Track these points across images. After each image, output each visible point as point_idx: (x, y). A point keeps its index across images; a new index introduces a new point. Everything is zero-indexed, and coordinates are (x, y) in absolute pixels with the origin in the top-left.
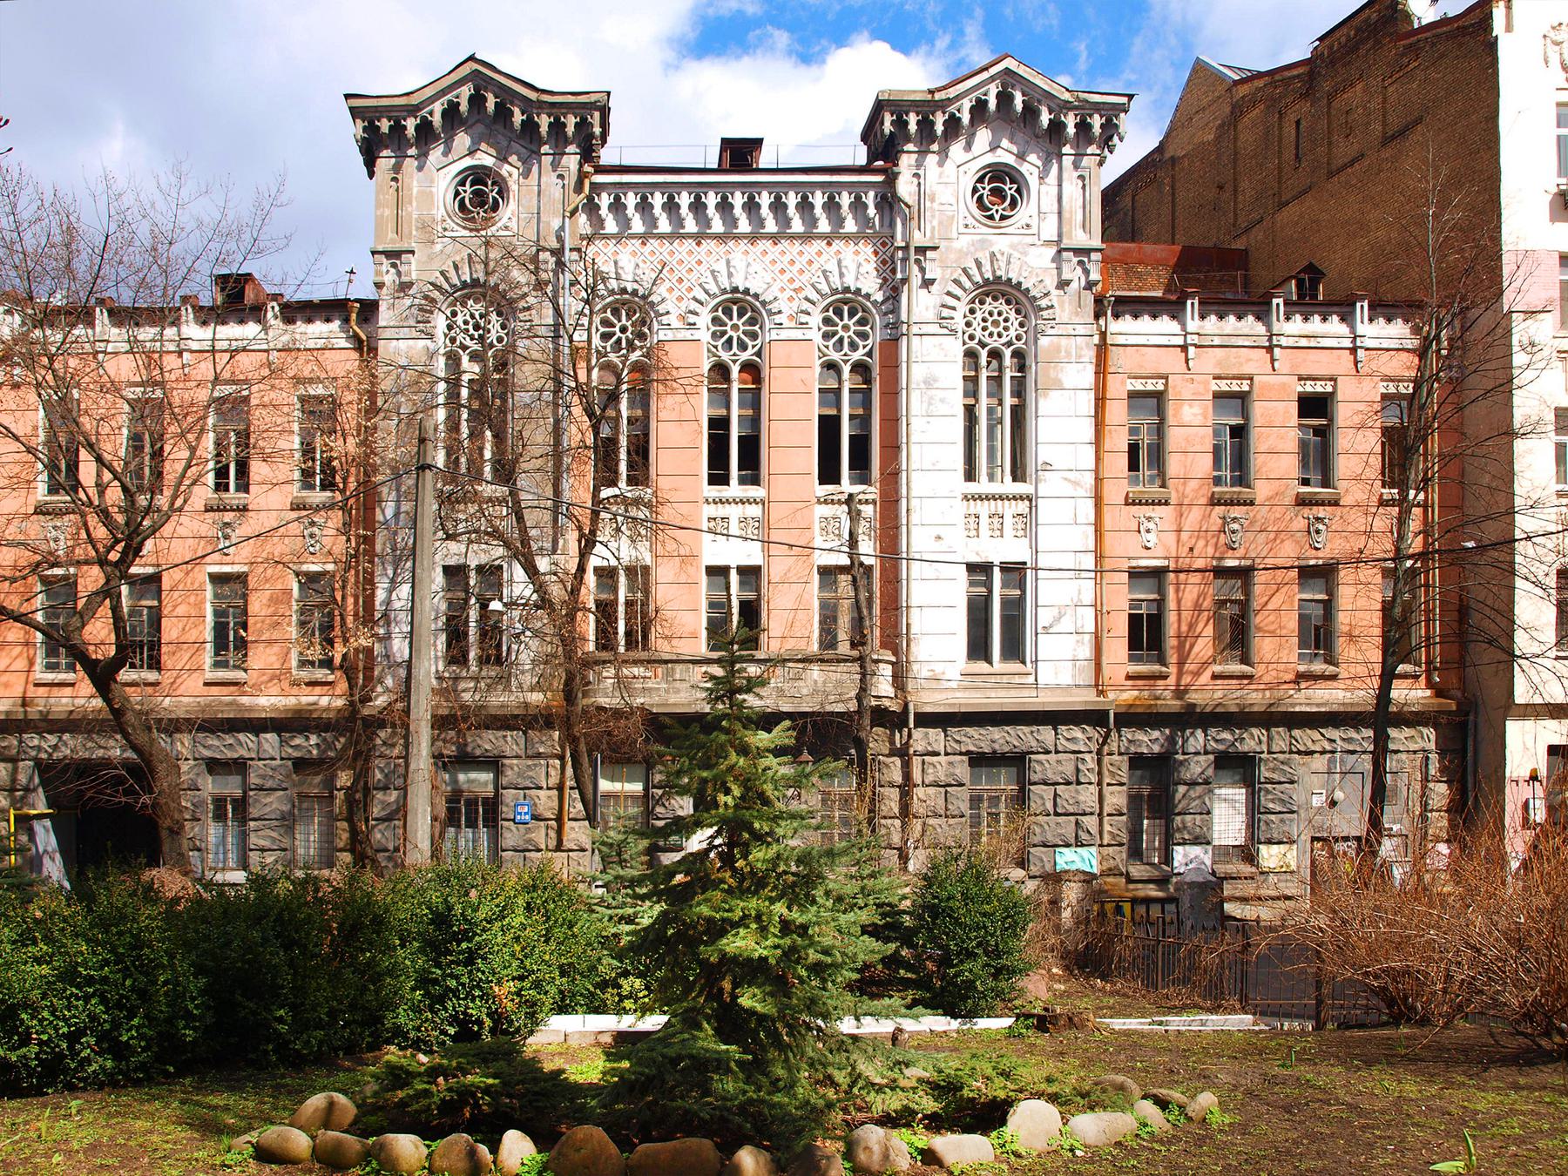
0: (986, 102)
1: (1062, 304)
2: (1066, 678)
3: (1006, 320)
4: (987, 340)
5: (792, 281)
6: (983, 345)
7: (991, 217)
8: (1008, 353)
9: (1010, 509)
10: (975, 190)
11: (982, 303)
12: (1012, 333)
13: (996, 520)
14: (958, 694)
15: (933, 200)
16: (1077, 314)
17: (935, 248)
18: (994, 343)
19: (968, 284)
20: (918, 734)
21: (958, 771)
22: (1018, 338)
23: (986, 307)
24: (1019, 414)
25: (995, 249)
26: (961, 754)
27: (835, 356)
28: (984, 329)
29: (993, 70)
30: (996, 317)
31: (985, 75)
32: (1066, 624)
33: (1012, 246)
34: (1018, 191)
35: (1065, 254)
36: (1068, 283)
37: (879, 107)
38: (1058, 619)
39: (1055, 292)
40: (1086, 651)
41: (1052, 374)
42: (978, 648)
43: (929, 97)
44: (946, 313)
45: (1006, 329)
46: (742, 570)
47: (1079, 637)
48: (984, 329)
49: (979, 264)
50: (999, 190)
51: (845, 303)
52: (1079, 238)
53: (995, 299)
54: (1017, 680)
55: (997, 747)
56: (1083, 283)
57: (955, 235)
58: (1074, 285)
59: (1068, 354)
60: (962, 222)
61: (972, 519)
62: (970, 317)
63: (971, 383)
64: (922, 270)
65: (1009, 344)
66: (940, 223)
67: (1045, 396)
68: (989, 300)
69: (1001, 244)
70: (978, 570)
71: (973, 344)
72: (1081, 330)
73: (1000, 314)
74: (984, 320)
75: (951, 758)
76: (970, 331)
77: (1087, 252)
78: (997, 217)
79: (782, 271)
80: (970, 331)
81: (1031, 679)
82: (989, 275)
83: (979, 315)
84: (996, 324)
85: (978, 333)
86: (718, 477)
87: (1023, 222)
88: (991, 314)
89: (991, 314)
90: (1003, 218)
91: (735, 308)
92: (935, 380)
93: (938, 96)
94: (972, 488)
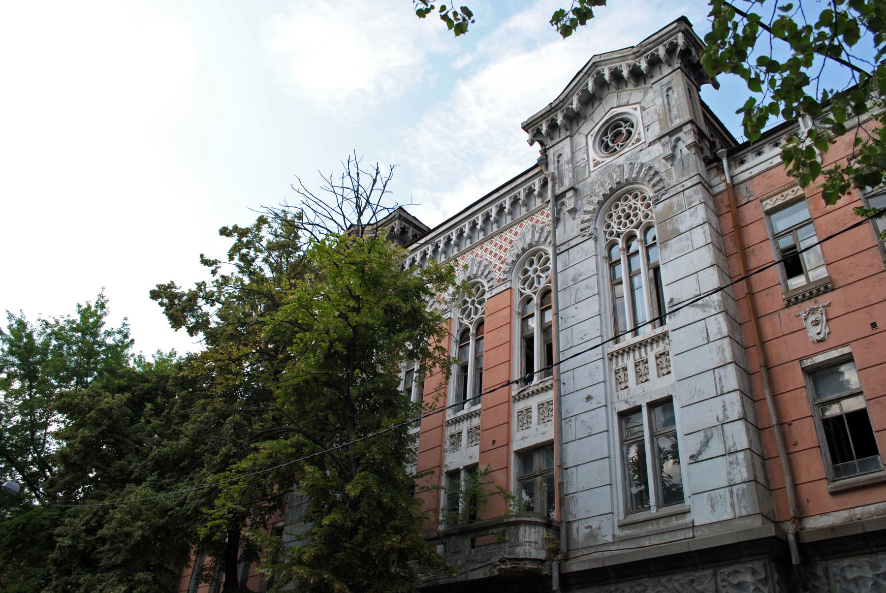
1: (670, 176)
3: (636, 208)
4: (623, 229)
8: (638, 232)
9: (651, 354)
11: (617, 206)
14: (612, 548)
16: (683, 175)
18: (630, 228)
22: (646, 216)
23: (620, 208)
27: (528, 292)
28: (619, 223)
29: (585, 71)
31: (581, 75)
32: (716, 447)
34: (632, 126)
38: (706, 443)
40: (742, 473)
47: (731, 458)
52: (677, 122)
53: (626, 199)
54: (675, 522)
56: (685, 151)
59: (680, 206)
62: (609, 221)
69: (621, 160)
71: (612, 238)
73: (630, 207)
74: (619, 217)
77: (679, 129)
80: (610, 230)
81: (688, 519)
83: (614, 217)
84: (628, 217)
87: (633, 141)
89: (624, 211)
92: (580, 275)
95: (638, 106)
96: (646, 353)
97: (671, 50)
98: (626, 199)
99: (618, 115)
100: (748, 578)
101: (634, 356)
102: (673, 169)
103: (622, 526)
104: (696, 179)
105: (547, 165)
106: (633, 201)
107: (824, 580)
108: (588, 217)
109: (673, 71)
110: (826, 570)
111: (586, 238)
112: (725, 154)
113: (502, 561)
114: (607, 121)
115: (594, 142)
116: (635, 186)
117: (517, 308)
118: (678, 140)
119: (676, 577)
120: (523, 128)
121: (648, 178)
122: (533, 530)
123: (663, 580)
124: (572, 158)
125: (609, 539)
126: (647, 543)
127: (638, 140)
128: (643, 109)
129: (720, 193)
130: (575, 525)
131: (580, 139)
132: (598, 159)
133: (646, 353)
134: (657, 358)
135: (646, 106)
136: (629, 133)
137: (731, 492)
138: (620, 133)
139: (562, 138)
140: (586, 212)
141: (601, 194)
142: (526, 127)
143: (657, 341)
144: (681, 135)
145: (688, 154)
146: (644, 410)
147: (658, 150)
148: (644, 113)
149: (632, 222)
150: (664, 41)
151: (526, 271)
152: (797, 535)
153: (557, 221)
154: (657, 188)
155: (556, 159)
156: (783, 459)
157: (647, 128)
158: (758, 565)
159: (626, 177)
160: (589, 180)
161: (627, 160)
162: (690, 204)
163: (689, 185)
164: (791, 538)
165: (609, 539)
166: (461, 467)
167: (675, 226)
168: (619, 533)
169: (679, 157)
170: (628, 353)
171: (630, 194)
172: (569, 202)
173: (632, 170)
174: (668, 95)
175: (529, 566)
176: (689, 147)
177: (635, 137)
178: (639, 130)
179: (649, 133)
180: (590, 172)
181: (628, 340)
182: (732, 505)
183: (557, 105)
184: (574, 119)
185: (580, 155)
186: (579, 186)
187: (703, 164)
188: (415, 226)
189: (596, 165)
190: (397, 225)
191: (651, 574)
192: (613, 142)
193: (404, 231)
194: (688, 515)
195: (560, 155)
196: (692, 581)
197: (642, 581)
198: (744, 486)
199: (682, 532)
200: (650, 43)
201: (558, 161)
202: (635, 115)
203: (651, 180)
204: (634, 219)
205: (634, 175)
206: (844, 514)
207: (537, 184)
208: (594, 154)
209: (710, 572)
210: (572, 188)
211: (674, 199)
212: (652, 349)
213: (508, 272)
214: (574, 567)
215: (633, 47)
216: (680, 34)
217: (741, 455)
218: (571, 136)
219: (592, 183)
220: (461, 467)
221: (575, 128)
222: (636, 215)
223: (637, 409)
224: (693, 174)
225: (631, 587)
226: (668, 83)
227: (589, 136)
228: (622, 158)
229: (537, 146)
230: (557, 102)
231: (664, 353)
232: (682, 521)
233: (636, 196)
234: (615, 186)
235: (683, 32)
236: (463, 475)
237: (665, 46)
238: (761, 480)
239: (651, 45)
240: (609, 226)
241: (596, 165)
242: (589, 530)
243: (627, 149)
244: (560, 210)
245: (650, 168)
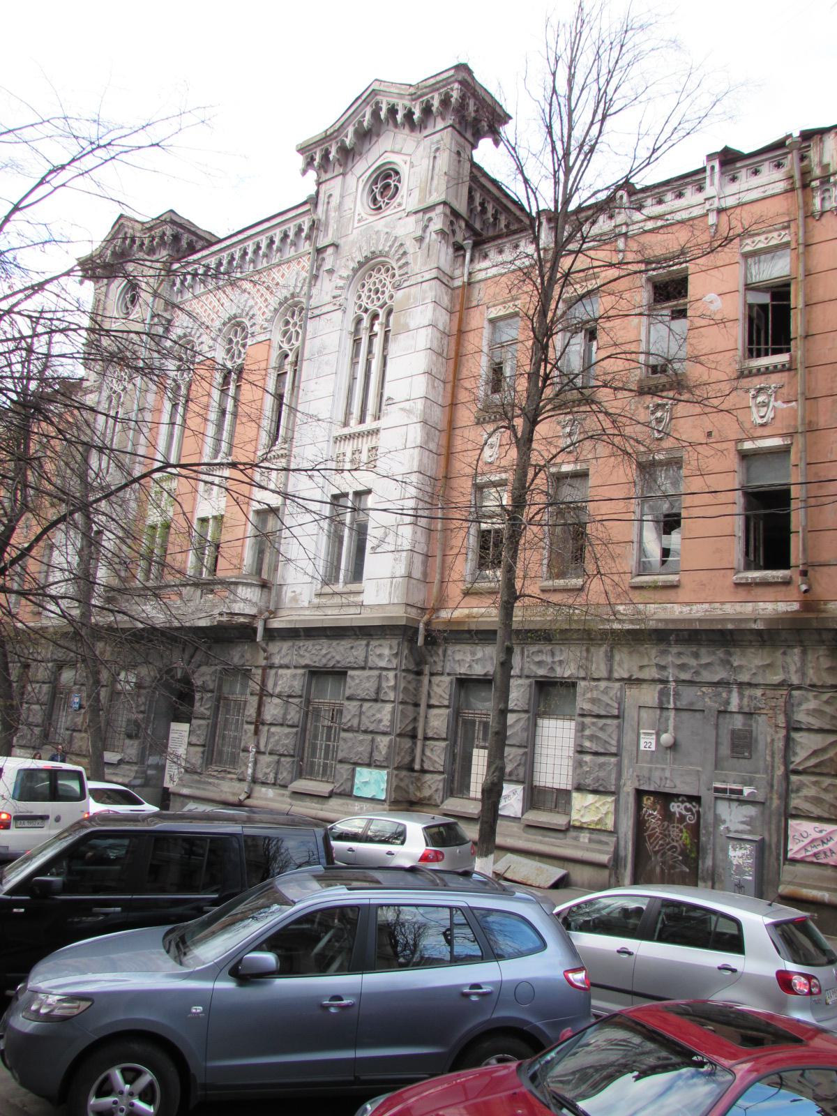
1: (415, 260)
2: (384, 600)
6: (366, 311)
8: (381, 312)
11: (371, 276)
17: (335, 246)
20: (274, 647)
22: (391, 297)
23: (373, 279)
31: (360, 102)
40: (401, 570)
43: (324, 135)
47: (397, 555)
56: (434, 236)
60: (357, 218)
63: (357, 342)
65: (381, 307)
70: (337, 499)
71: (359, 312)
72: (427, 276)
73: (381, 281)
74: (370, 290)
81: (358, 599)
83: (366, 288)
84: (377, 292)
90: (387, 204)
93: (328, 133)
95: (408, 158)
97: (445, 102)
98: (379, 270)
100: (386, 652)
102: (419, 254)
103: (319, 595)
104: (434, 273)
105: (316, 205)
107: (442, 658)
108: (341, 283)
110: (445, 651)
111: (336, 307)
112: (470, 246)
113: (221, 614)
114: (379, 168)
115: (363, 190)
116: (387, 260)
117: (274, 362)
119: (343, 643)
120: (298, 151)
121: (396, 257)
122: (249, 590)
123: (335, 643)
124: (341, 204)
125: (306, 604)
127: (400, 205)
128: (412, 165)
129: (458, 287)
130: (285, 588)
131: (351, 180)
135: (415, 163)
137: (392, 583)
138: (387, 186)
139: (336, 173)
140: (341, 277)
141: (357, 260)
142: (302, 150)
144: (432, 214)
145: (436, 240)
146: (351, 497)
148: (412, 170)
150: (441, 88)
151: (287, 323)
152: (428, 624)
153: (316, 277)
155: (326, 200)
156: (438, 559)
158: (395, 642)
159: (380, 248)
160: (351, 238)
161: (386, 226)
162: (424, 299)
164: (421, 626)
165: (306, 604)
168: (316, 601)
169: (427, 240)
171: (383, 266)
172: (329, 258)
173: (386, 240)
174: (435, 157)
175: (242, 620)
176: (437, 232)
177: (398, 199)
179: (410, 199)
180: (353, 229)
181: (354, 427)
182: (390, 594)
183: (332, 134)
184: (348, 155)
185: (348, 203)
186: (341, 242)
187: (451, 250)
188: (190, 231)
189: (359, 221)
190: (169, 230)
191: (328, 637)
192: (382, 194)
193: (176, 238)
195: (331, 195)
196: (352, 648)
197: (321, 641)
198: (401, 579)
200: (426, 87)
201: (328, 203)
202: (404, 170)
203: (399, 259)
205: (387, 249)
206: (466, 611)
207: (306, 223)
209: (364, 642)
210: (333, 245)
211: (413, 289)
214: (275, 624)
215: (411, 86)
216: (456, 85)
217: (404, 554)
218: (344, 174)
221: (350, 165)
222: (383, 293)
223: (345, 495)
225: (313, 645)
226: (438, 142)
228: (382, 222)
229: (312, 174)
230: (332, 130)
232: (352, 599)
233: (388, 270)
234: (369, 255)
235: (460, 82)
236: (211, 522)
237: (440, 94)
238: (417, 573)
240: (360, 297)
241: (359, 221)
243: (388, 212)
244: (321, 265)
245: (402, 245)
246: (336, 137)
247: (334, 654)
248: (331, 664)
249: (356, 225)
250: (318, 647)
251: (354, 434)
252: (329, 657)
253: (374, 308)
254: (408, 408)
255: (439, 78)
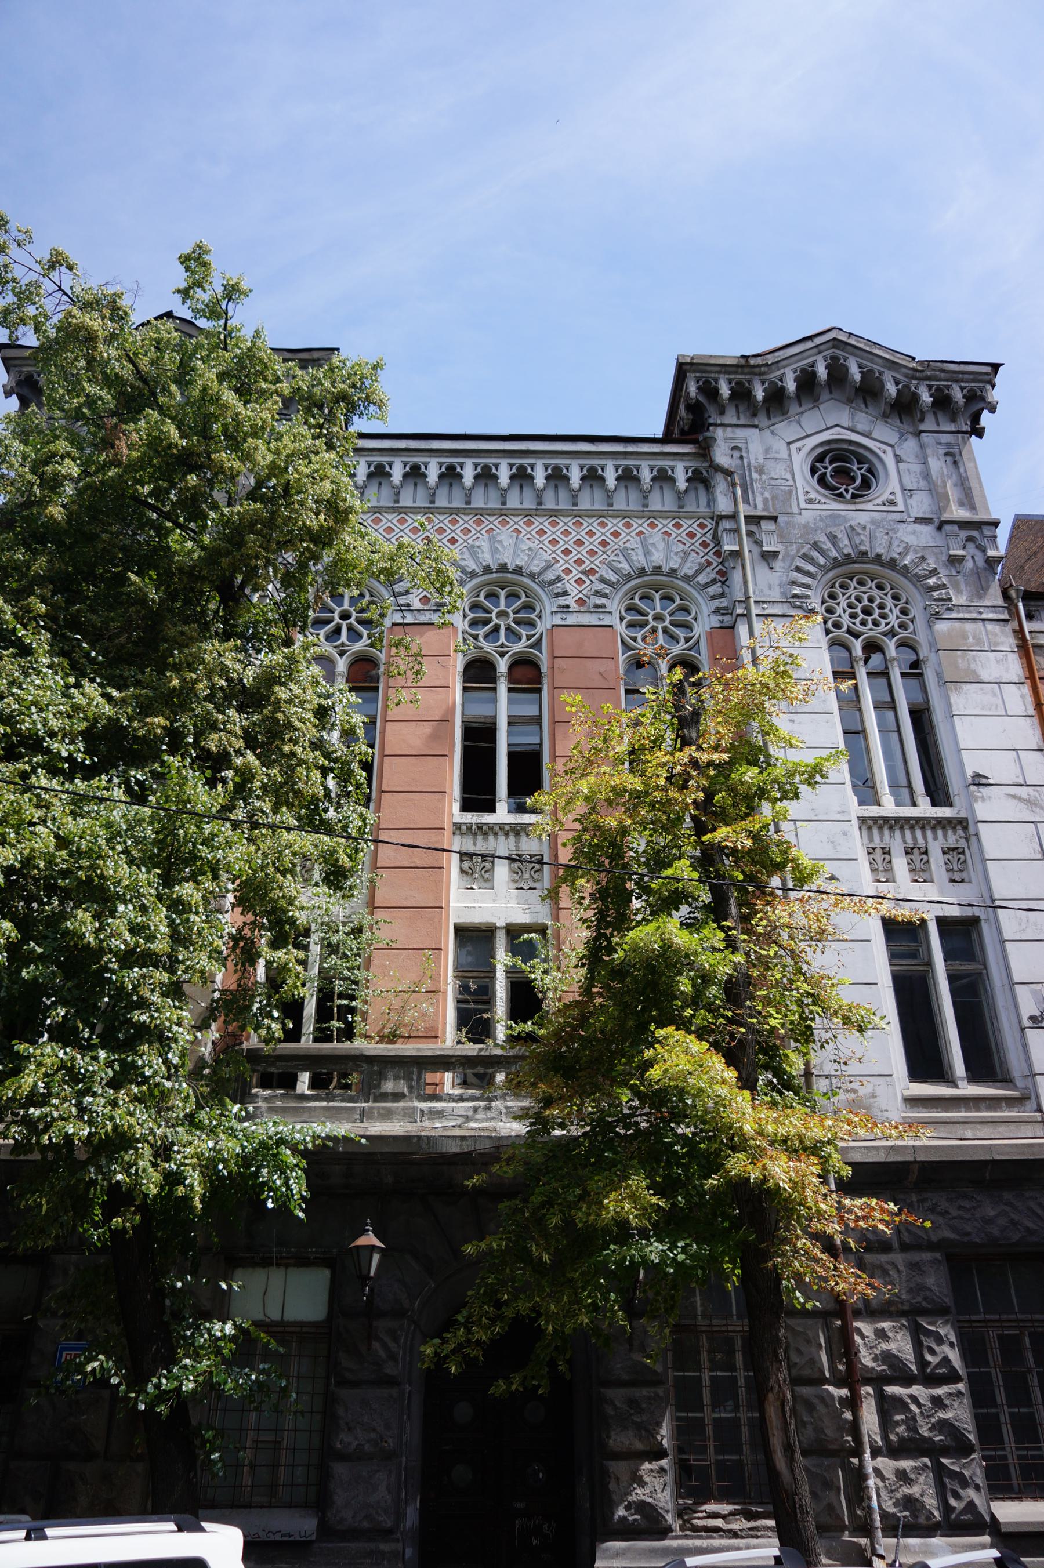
0: (814, 374)
3: (881, 607)
4: (861, 629)
5: (579, 562)
7: (841, 495)
8: (891, 646)
10: (813, 470)
12: (893, 620)
13: (916, 856)
15: (761, 471)
17: (775, 519)
18: (869, 632)
19: (822, 561)
21: (930, 1281)
24: (921, 718)
25: (853, 523)
26: (931, 1247)
30: (866, 602)
31: (810, 344)
33: (873, 522)
35: (947, 528)
36: (960, 559)
37: (683, 370)
39: (943, 572)
41: (962, 664)
42: (924, 1059)
43: (743, 361)
44: (797, 591)
45: (884, 616)
46: (513, 931)
48: (853, 616)
49: (833, 538)
50: (843, 470)
51: (651, 586)
53: (861, 583)
55: (995, 1231)
57: (795, 510)
58: (969, 564)
59: (978, 641)
61: (878, 855)
62: (831, 603)
64: (759, 543)
66: (774, 498)
67: (958, 691)
68: (853, 584)
69: (863, 518)
71: (841, 633)
73: (871, 600)
74: (850, 606)
75: (916, 1256)
76: (834, 618)
78: (848, 496)
79: (567, 552)
82: (848, 550)
83: (843, 601)
84: (867, 612)
85: (846, 621)
86: (477, 794)
88: (859, 600)
91: (503, 594)
93: (752, 362)
94: (872, 811)
95: (889, 449)
96: (925, 837)
99: (851, 442)
101: (903, 837)
106: (879, 592)
109: (958, 432)
114: (828, 442)
116: (888, 572)
118: (970, 539)
123: (1007, 1196)
126: (969, 1135)
132: (813, 495)
133: (925, 837)
134: (944, 853)
135: (904, 457)
136: (866, 485)
143: (944, 828)
144: (975, 533)
147: (925, 535)
148: (902, 466)
149: (876, 624)
154: (936, 594)
157: (908, 493)
159: (880, 550)
162: (996, 644)
163: (991, 616)
166: (500, 923)
167: (972, 666)
170: (891, 828)
178: (889, 486)
179: (913, 502)
183: (758, 366)
194: (1028, 1103)
199: (1029, 1127)
200: (943, 371)
203: (927, 577)
204: (883, 622)
208: (804, 483)
211: (968, 626)
212: (935, 838)
213: (606, 596)
215: (913, 359)
219: (806, 526)
220: (500, 923)
222: (884, 616)
224: (995, 604)
227: (793, 447)
230: (759, 361)
231: (954, 849)
239: (943, 375)
241: (810, 501)
242: (852, 1096)
243: (869, 506)
246: (764, 374)
247: (1015, 1217)
248: (1015, 1237)
249: (803, 505)
250: (966, 1204)
251: (886, 820)
252: (1002, 1221)
253: (871, 633)
254: (1025, 796)
255: (962, 368)
